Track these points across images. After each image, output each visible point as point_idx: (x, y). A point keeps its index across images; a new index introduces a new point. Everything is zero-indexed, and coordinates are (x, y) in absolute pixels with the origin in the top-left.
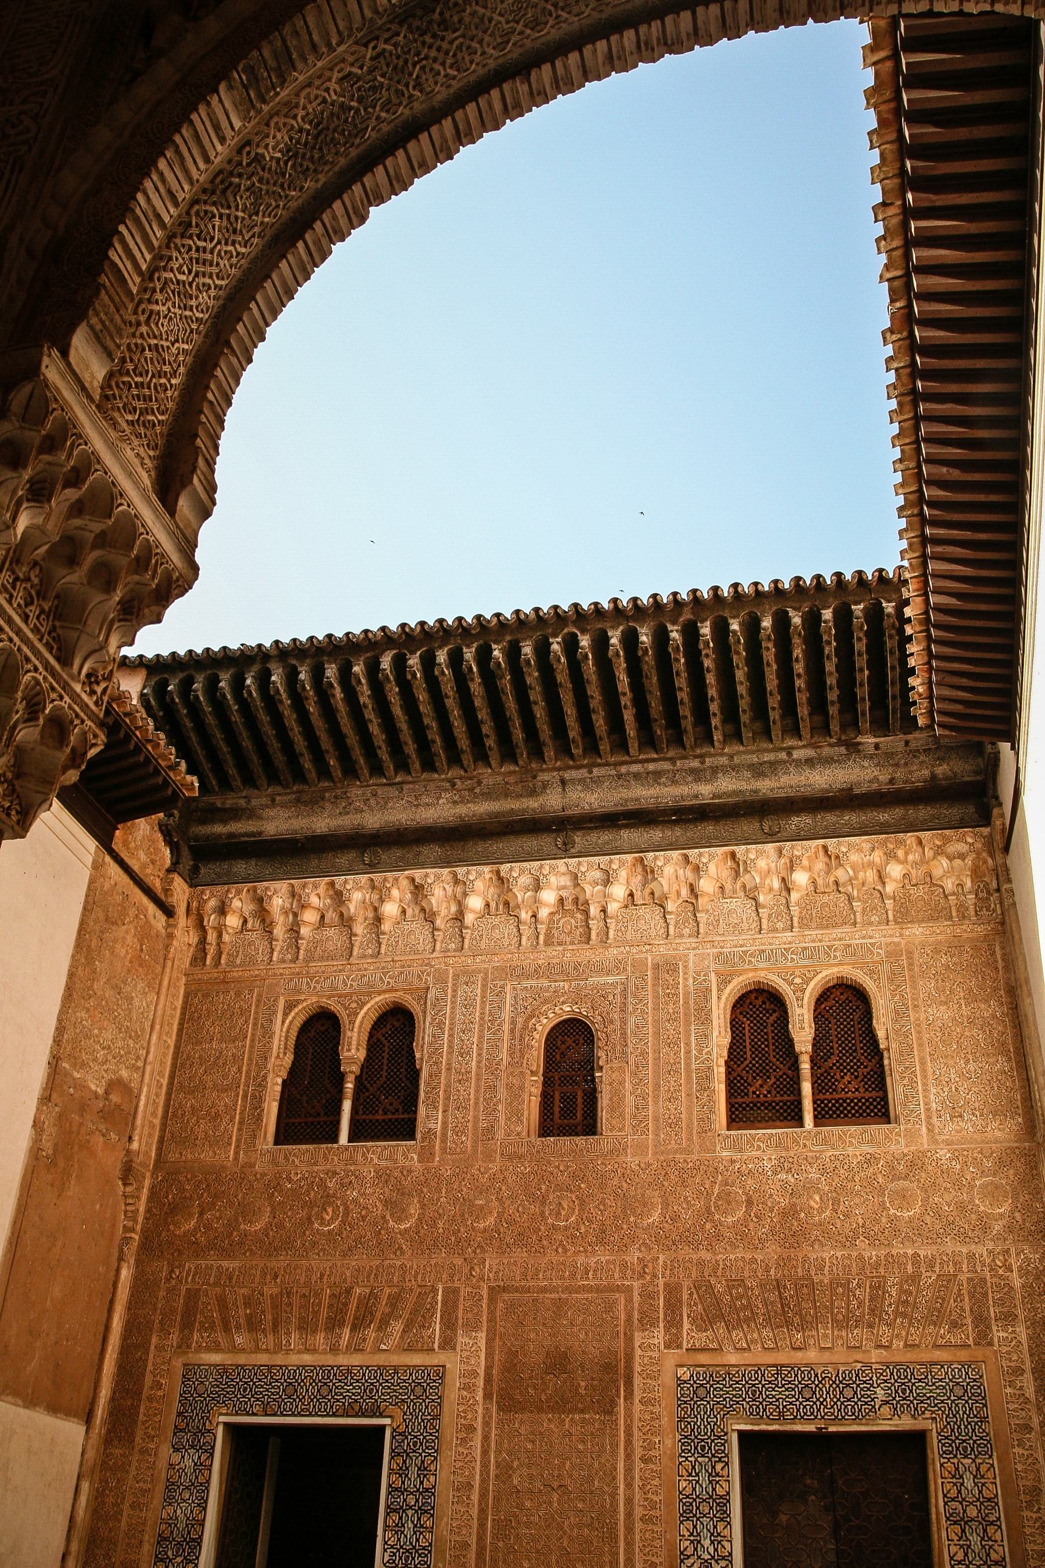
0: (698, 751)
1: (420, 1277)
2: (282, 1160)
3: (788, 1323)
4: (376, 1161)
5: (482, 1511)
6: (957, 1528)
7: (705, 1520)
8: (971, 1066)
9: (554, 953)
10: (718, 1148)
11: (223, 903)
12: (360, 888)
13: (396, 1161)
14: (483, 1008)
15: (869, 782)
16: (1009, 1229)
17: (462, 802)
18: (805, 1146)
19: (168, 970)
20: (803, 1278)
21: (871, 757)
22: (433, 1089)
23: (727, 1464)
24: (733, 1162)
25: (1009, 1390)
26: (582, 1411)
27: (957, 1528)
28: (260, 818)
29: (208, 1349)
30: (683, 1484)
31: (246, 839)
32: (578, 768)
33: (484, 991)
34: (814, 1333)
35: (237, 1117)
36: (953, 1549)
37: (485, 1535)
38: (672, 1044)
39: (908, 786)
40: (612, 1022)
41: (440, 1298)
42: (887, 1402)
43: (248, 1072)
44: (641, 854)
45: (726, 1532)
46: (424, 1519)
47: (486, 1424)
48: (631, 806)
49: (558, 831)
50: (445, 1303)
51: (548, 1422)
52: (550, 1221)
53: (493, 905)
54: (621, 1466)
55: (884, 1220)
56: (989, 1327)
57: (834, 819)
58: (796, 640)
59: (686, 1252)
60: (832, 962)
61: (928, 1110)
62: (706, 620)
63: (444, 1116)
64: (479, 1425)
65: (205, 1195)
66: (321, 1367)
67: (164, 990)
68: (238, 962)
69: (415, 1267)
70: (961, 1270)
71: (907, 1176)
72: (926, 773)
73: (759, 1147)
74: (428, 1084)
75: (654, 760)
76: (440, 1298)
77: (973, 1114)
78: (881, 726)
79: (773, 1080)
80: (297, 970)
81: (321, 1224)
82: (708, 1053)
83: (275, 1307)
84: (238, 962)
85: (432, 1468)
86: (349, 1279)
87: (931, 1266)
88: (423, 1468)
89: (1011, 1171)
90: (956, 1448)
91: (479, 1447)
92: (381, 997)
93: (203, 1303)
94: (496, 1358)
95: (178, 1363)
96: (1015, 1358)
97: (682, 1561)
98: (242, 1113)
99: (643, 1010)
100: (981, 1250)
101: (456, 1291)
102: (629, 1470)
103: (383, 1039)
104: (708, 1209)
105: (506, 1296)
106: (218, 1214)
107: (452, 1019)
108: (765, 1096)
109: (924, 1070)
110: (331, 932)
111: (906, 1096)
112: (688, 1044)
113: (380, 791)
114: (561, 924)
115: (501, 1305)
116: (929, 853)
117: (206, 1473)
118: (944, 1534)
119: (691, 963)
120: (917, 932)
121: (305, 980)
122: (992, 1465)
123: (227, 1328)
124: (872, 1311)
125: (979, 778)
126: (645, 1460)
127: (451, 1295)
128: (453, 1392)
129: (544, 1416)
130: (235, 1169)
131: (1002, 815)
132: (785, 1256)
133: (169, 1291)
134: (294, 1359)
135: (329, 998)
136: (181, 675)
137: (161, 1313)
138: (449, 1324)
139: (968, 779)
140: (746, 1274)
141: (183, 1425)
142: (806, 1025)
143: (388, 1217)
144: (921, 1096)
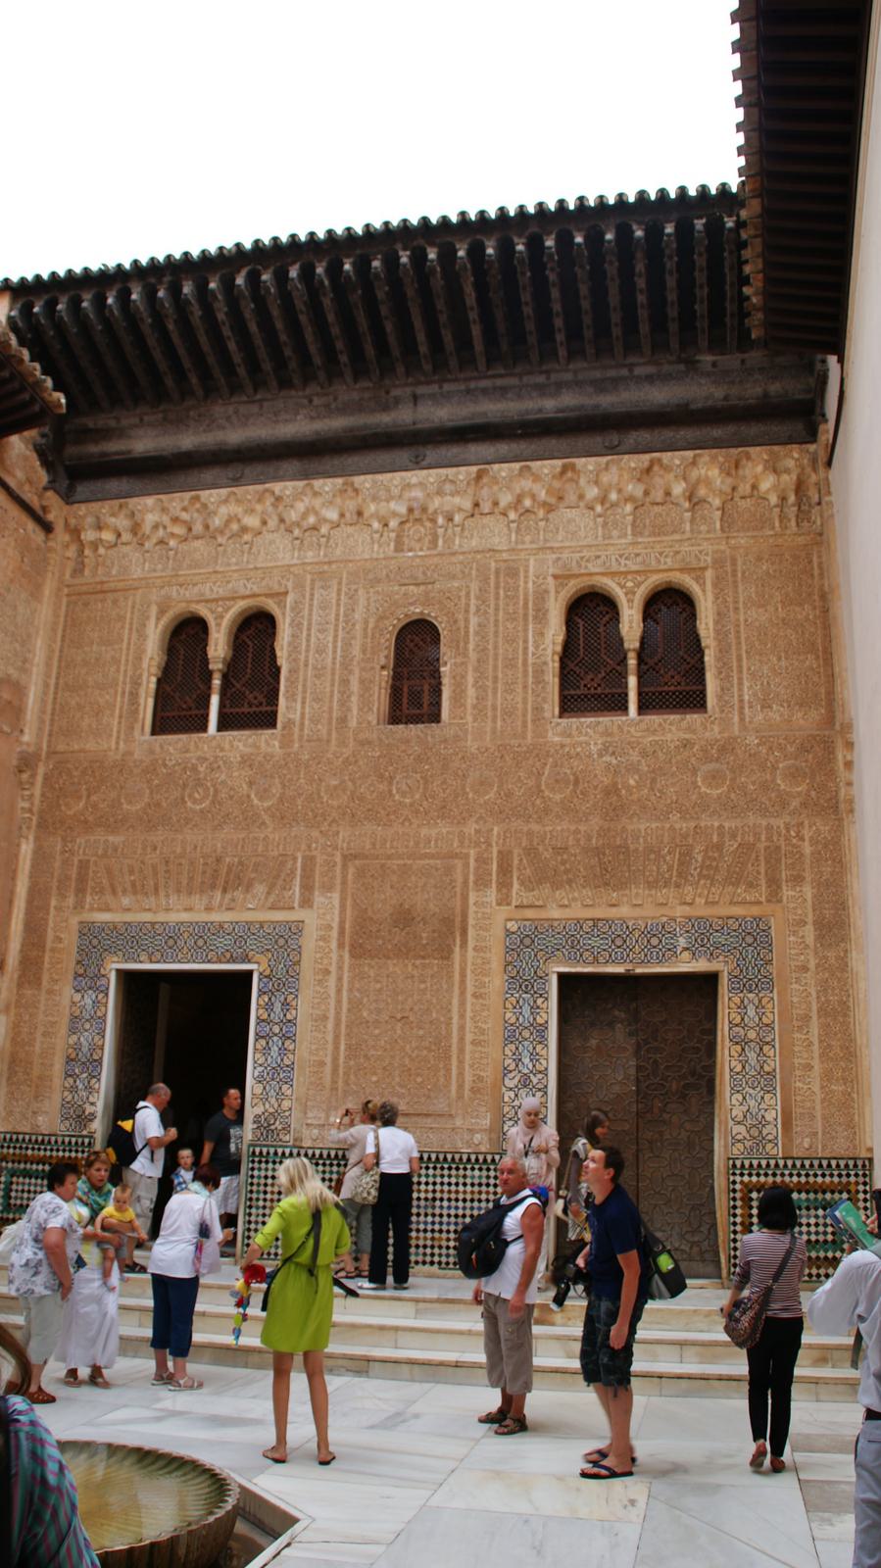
0: (544, 368)
1: (281, 847)
2: (158, 749)
3: (607, 884)
4: (241, 748)
5: (337, 1037)
6: (739, 1048)
7: (526, 1043)
8: (783, 663)
10: (550, 734)
11: (98, 518)
12: (226, 501)
13: (258, 748)
14: (338, 610)
15: (707, 398)
16: (804, 805)
17: (318, 417)
18: (629, 732)
20: (620, 846)
21: (708, 374)
22: (292, 682)
23: (547, 999)
24: (563, 746)
25: (792, 938)
26: (423, 958)
27: (739, 1048)
28: (130, 437)
29: (100, 910)
30: (508, 1015)
31: (117, 457)
32: (428, 383)
33: (339, 594)
34: (627, 892)
35: (117, 711)
36: (733, 1063)
37: (338, 1054)
38: (511, 640)
39: (742, 403)
40: (455, 622)
41: (299, 864)
42: (687, 949)
43: (126, 671)
44: (487, 466)
45: (544, 1052)
46: (287, 1043)
47: (340, 968)
48: (478, 421)
49: (410, 444)
50: (303, 870)
51: (394, 967)
52: (397, 797)
53: (348, 515)
54: (455, 1001)
55: (694, 797)
57: (672, 434)
58: (639, 255)
59: (517, 824)
60: (662, 567)
61: (741, 701)
62: (551, 233)
63: (303, 708)
64: (333, 969)
66: (197, 923)
67: (45, 599)
68: (114, 572)
70: (759, 839)
71: (717, 760)
72: (759, 390)
73: (587, 734)
74: (287, 680)
75: (501, 376)
76: (299, 864)
77: (782, 706)
78: (717, 345)
79: (603, 674)
80: (167, 579)
81: (194, 803)
82: (544, 649)
83: (155, 873)
85: (294, 1003)
86: (219, 850)
87: (734, 836)
88: (286, 1004)
89: (810, 756)
90: (742, 984)
95: (74, 921)
96: (800, 912)
97: (505, 1075)
98: (121, 708)
99: (486, 612)
100: (779, 823)
101: (313, 858)
102: (463, 1003)
103: (247, 640)
104: (539, 786)
105: (357, 862)
107: (310, 620)
108: (595, 689)
109: (740, 667)
110: (197, 544)
111: (722, 689)
112: (526, 641)
113: (243, 409)
115: (351, 870)
116: (760, 468)
117: (103, 1009)
118: (727, 1052)
119: (531, 570)
120: (742, 540)
122: (772, 999)
123: (114, 892)
124: (680, 875)
125: (809, 396)
126: (475, 996)
128: (309, 943)
129: (389, 962)
130: (119, 757)
131: (827, 431)
132: (606, 827)
133: (65, 862)
134: (173, 917)
136: (46, 297)
137: (59, 881)
138: (307, 887)
139: (797, 397)
140: (570, 843)
141: (81, 971)
142: (634, 625)
143: (253, 796)
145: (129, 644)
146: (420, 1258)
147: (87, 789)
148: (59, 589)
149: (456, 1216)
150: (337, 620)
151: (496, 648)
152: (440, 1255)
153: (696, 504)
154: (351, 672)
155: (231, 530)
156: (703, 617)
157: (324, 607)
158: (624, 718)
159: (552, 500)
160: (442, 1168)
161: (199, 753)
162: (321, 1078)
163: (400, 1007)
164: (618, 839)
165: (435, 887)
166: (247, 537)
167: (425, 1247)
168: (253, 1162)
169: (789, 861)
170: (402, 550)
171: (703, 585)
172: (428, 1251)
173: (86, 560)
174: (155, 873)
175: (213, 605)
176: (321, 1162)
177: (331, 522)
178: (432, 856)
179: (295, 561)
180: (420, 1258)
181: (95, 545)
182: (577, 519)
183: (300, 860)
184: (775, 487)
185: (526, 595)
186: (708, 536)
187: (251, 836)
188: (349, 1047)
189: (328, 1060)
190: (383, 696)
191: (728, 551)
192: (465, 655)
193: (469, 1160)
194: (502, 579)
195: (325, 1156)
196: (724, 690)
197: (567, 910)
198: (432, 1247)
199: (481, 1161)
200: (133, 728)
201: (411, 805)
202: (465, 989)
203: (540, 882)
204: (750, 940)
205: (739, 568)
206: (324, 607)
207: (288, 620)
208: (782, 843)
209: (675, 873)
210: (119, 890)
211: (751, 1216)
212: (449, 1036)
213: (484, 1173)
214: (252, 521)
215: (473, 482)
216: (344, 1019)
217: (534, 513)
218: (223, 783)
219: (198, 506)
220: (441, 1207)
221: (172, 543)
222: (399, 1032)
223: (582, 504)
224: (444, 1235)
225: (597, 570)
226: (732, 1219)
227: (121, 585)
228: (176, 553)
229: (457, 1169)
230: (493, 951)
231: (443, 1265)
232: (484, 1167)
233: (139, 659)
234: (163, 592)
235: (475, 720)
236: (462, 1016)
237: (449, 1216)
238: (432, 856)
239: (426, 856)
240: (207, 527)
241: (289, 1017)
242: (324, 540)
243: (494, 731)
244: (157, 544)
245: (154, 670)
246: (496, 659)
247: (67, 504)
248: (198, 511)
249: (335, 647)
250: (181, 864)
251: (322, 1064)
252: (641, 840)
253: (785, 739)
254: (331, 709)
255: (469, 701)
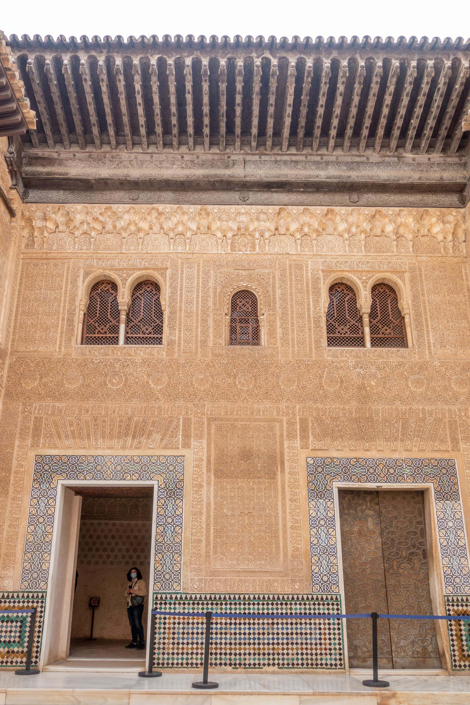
1: (169, 412)
2: (87, 353)
4: (142, 354)
5: (208, 525)
9: (237, 255)
10: (325, 355)
11: (45, 213)
13: (153, 355)
14: (198, 281)
18: (369, 356)
19: (12, 247)
20: (368, 418)
24: (333, 362)
26: (259, 478)
33: (198, 272)
34: (374, 443)
35: (59, 329)
40: (268, 292)
41: (181, 423)
43: (64, 306)
47: (209, 484)
50: (183, 426)
52: (239, 386)
53: (202, 228)
54: (280, 503)
55: (408, 393)
56: (458, 443)
60: (381, 270)
61: (429, 343)
63: (180, 334)
64: (204, 484)
65: (43, 369)
68: (54, 248)
69: (166, 407)
71: (418, 374)
73: (346, 356)
74: (169, 317)
76: (181, 423)
77: (451, 346)
80: (91, 254)
83: (88, 426)
84: (54, 248)
87: (431, 415)
91: (205, 494)
92: (140, 272)
93: (45, 424)
94: (213, 452)
98: (62, 328)
100: (455, 408)
101: (190, 419)
102: (284, 505)
104: (321, 383)
106: (51, 379)
109: (427, 325)
111: (418, 336)
112: (309, 305)
114: (239, 241)
116: (434, 220)
119: (310, 266)
121: (95, 260)
124: (403, 434)
126: (291, 500)
127: (187, 422)
129: (238, 480)
135: (110, 270)
138: (187, 436)
142: (368, 299)
143: (150, 383)
144: (426, 336)
145: (66, 290)
146: (266, 662)
147: (40, 374)
148: (18, 255)
149: (287, 634)
150: (198, 286)
151: (292, 307)
152: (278, 659)
153: (398, 237)
154: (208, 315)
155: (130, 230)
156: (405, 298)
157: (190, 278)
158: (366, 349)
159: (321, 230)
160: (277, 604)
161: (115, 357)
162: (199, 550)
163: (246, 507)
164: (367, 414)
165: (264, 437)
166: (141, 235)
167: (269, 654)
168: (156, 604)
169: (462, 429)
170: (235, 250)
171: (404, 281)
172: (271, 657)
173: (35, 239)
174: (88, 426)
175: (120, 273)
176: (201, 602)
177: (193, 231)
178: (261, 420)
179: (172, 251)
180: (266, 662)
181: (42, 230)
182: (334, 241)
183: (181, 420)
184: (442, 231)
185: (307, 280)
186: (406, 254)
187: (150, 405)
188: (216, 531)
189: (204, 539)
190: (227, 330)
191: (417, 263)
192: (274, 310)
193: (293, 598)
194: (293, 271)
195: (203, 599)
196: (420, 336)
197: (341, 452)
198: (273, 654)
199: (300, 599)
200: (71, 340)
201: (248, 391)
202: (285, 496)
203: (325, 436)
204: (444, 471)
205: (423, 273)
206: (190, 278)
207: (168, 284)
208: (457, 419)
209: (400, 434)
210: (63, 436)
211: (461, 630)
212: (277, 524)
213: (303, 606)
214: (144, 225)
215: (276, 215)
216: (212, 514)
217: (310, 236)
218: (131, 374)
219: (109, 213)
220: (278, 629)
221: (93, 234)
222: (246, 521)
223: (336, 233)
224: (280, 646)
225: (346, 269)
226: (450, 633)
227: (59, 255)
228: (95, 240)
229: (286, 604)
230: (301, 474)
231: (281, 666)
232: (303, 603)
233: (73, 300)
234: (88, 262)
235: (282, 346)
236: (284, 512)
237: (283, 634)
238: (261, 420)
239: (257, 420)
240: (115, 227)
241: (178, 513)
242: (189, 240)
243: (293, 353)
244: (82, 234)
245: (83, 307)
246: (292, 313)
247: (23, 203)
248: (109, 216)
249: (198, 301)
250: (104, 421)
251: (200, 541)
252: (380, 414)
253: (454, 364)
254: (197, 335)
255: (278, 335)
